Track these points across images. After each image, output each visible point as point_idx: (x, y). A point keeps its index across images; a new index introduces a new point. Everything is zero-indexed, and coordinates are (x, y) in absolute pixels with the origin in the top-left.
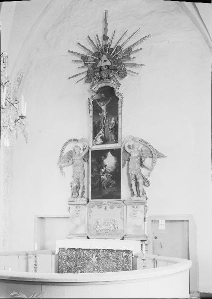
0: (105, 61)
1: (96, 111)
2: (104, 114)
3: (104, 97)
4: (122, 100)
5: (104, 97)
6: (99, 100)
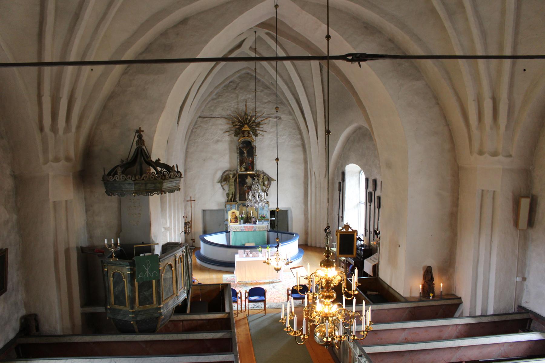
0: (246, 128)
1: (241, 153)
2: (246, 155)
3: (245, 146)
4: (256, 149)
5: (245, 146)
6: (242, 147)
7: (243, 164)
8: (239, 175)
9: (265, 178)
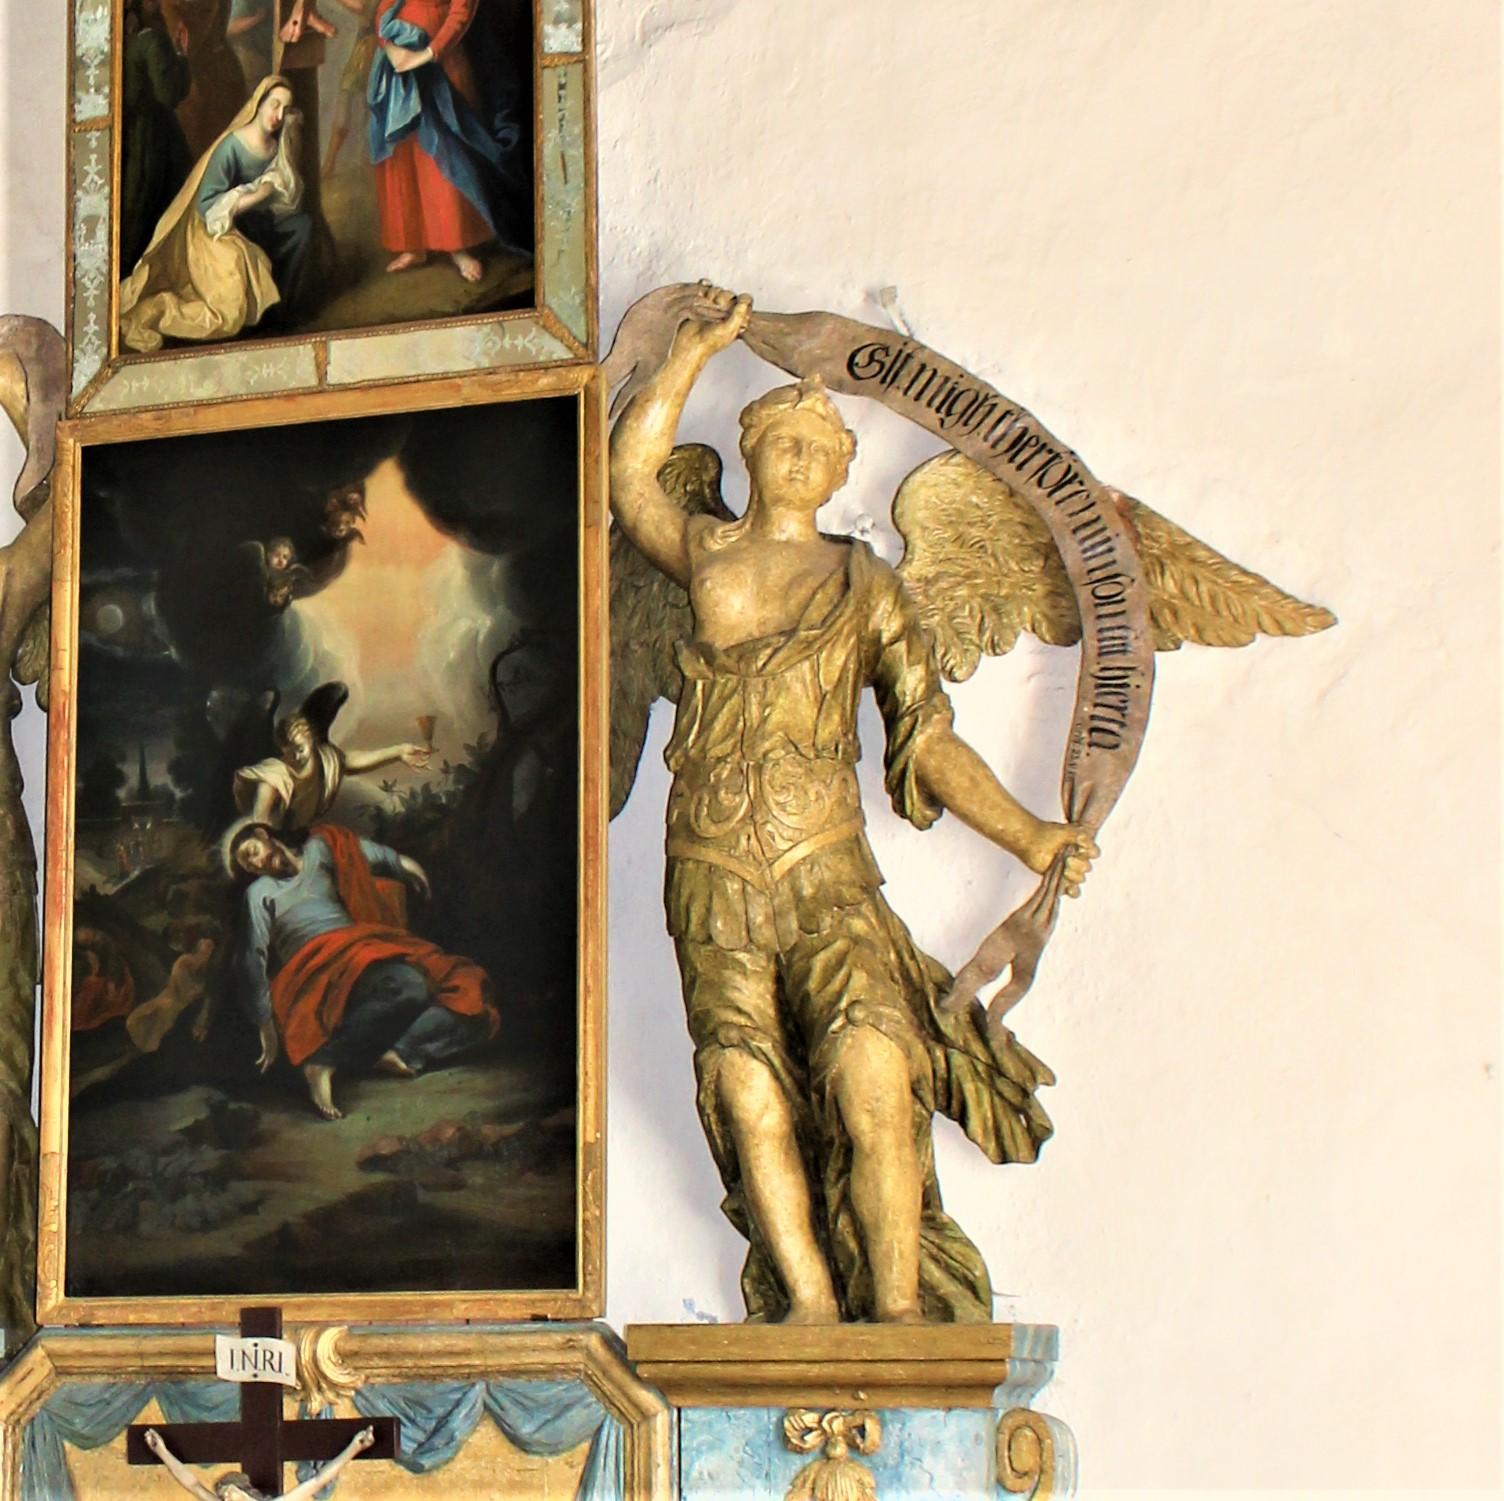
7: (231, 100)
8: (93, 457)
9: (955, 519)
